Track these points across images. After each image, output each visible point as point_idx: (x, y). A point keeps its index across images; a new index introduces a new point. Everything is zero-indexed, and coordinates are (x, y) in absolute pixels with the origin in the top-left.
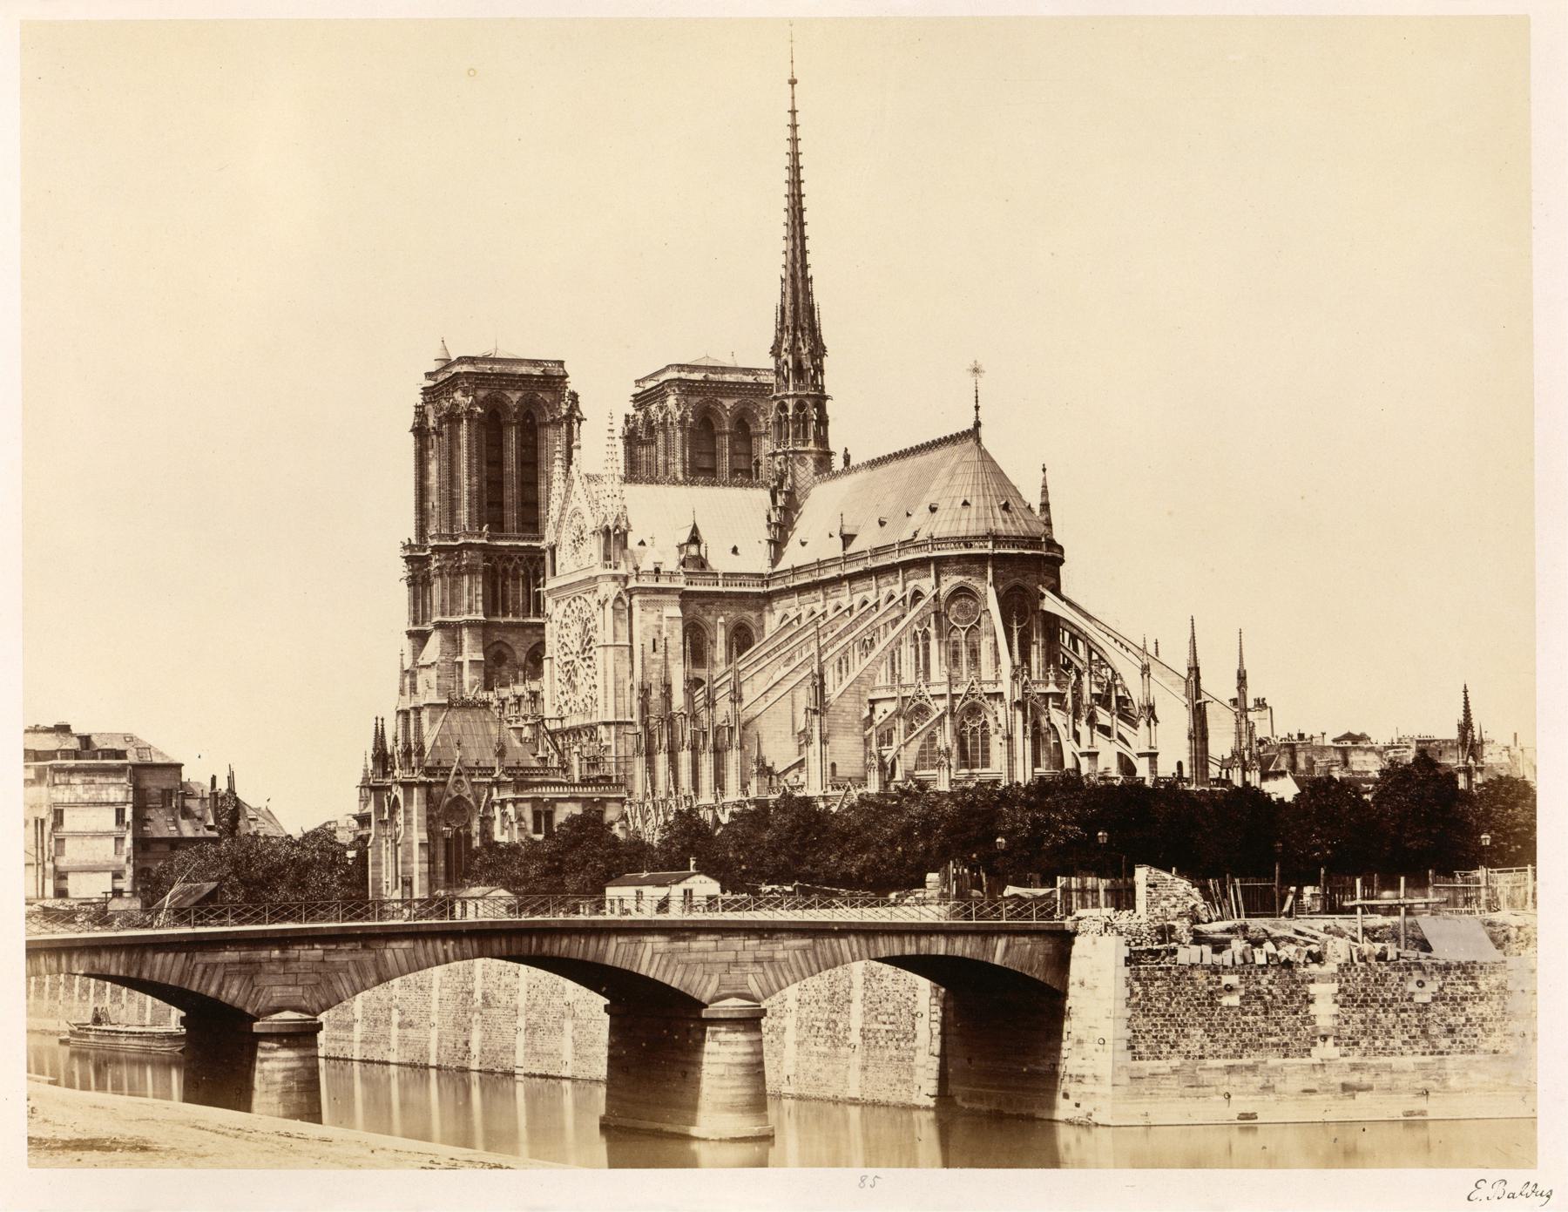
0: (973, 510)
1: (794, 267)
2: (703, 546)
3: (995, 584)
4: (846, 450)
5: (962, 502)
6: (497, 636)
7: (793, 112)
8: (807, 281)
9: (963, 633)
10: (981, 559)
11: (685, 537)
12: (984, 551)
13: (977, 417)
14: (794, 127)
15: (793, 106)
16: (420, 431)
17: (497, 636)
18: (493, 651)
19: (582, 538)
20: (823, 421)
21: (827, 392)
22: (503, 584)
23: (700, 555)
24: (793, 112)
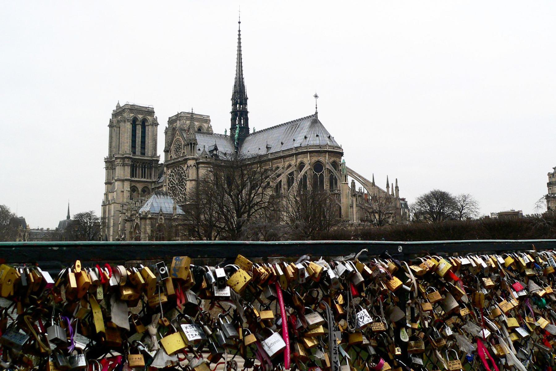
0: (320, 138)
3: (329, 160)
4: (254, 128)
5: (316, 135)
6: (133, 184)
7: (239, 31)
8: (243, 79)
9: (318, 176)
11: (213, 148)
12: (326, 149)
13: (316, 110)
16: (111, 126)
17: (133, 184)
19: (180, 148)
20: (246, 120)
21: (248, 111)
22: (136, 170)
24: (239, 31)
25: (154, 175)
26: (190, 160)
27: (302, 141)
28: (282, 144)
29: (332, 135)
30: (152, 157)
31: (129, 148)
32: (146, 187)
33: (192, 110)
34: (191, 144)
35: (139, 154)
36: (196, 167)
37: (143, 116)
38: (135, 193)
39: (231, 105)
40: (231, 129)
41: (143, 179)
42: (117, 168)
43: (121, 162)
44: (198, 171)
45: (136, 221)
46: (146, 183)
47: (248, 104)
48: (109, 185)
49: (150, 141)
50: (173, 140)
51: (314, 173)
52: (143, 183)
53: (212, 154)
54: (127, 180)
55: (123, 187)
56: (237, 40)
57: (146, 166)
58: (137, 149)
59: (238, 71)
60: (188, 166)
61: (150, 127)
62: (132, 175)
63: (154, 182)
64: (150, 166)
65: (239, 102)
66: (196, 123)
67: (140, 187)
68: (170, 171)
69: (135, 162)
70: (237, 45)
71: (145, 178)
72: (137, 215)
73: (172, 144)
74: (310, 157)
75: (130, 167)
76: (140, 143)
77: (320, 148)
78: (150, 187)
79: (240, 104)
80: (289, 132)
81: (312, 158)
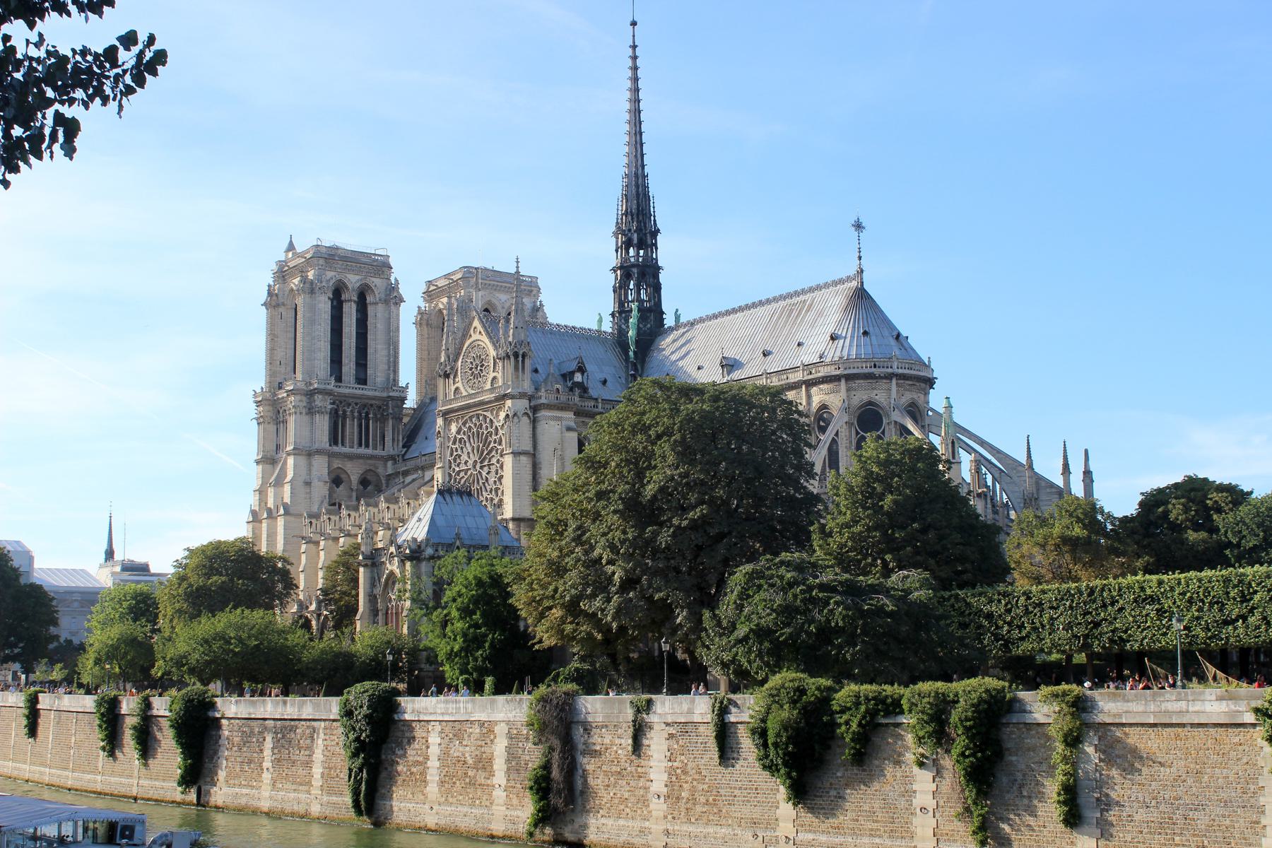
0: (873, 338)
1: (636, 167)
2: (585, 374)
4: (677, 310)
6: (337, 463)
7: (634, 47)
10: (889, 377)
11: (573, 366)
12: (890, 370)
14: (635, 58)
15: (634, 42)
17: (337, 463)
18: (333, 476)
20: (657, 288)
22: (344, 426)
23: (583, 382)
24: (634, 47)
25: (393, 440)
26: (512, 397)
27: (821, 348)
28: (765, 354)
29: (904, 334)
30: (386, 388)
31: (325, 365)
32: (370, 470)
33: (518, 262)
34: (516, 355)
35: (352, 379)
36: (529, 417)
37: (360, 277)
38: (341, 487)
39: (615, 248)
40: (613, 315)
41: (362, 450)
42: (292, 421)
43: (305, 404)
44: (534, 428)
45: (388, 565)
46: (369, 462)
47: (659, 245)
48: (269, 467)
49: (379, 347)
50: (462, 344)
51: (857, 433)
52: (361, 461)
53: (569, 384)
54: (319, 452)
55: (310, 470)
56: (629, 73)
57: (371, 416)
58: (345, 369)
59: (632, 157)
60: (507, 415)
61: (380, 307)
62: (334, 440)
63: (392, 458)
64: (382, 415)
65: (635, 241)
66: (503, 297)
67: (354, 472)
68: (454, 428)
69: (341, 402)
70: (629, 84)
71: (367, 446)
72: (392, 549)
73: (459, 354)
74: (848, 390)
75: (327, 417)
76: (353, 352)
77: (875, 366)
78: (380, 471)
79: (639, 246)
80: (782, 322)
81: (854, 393)
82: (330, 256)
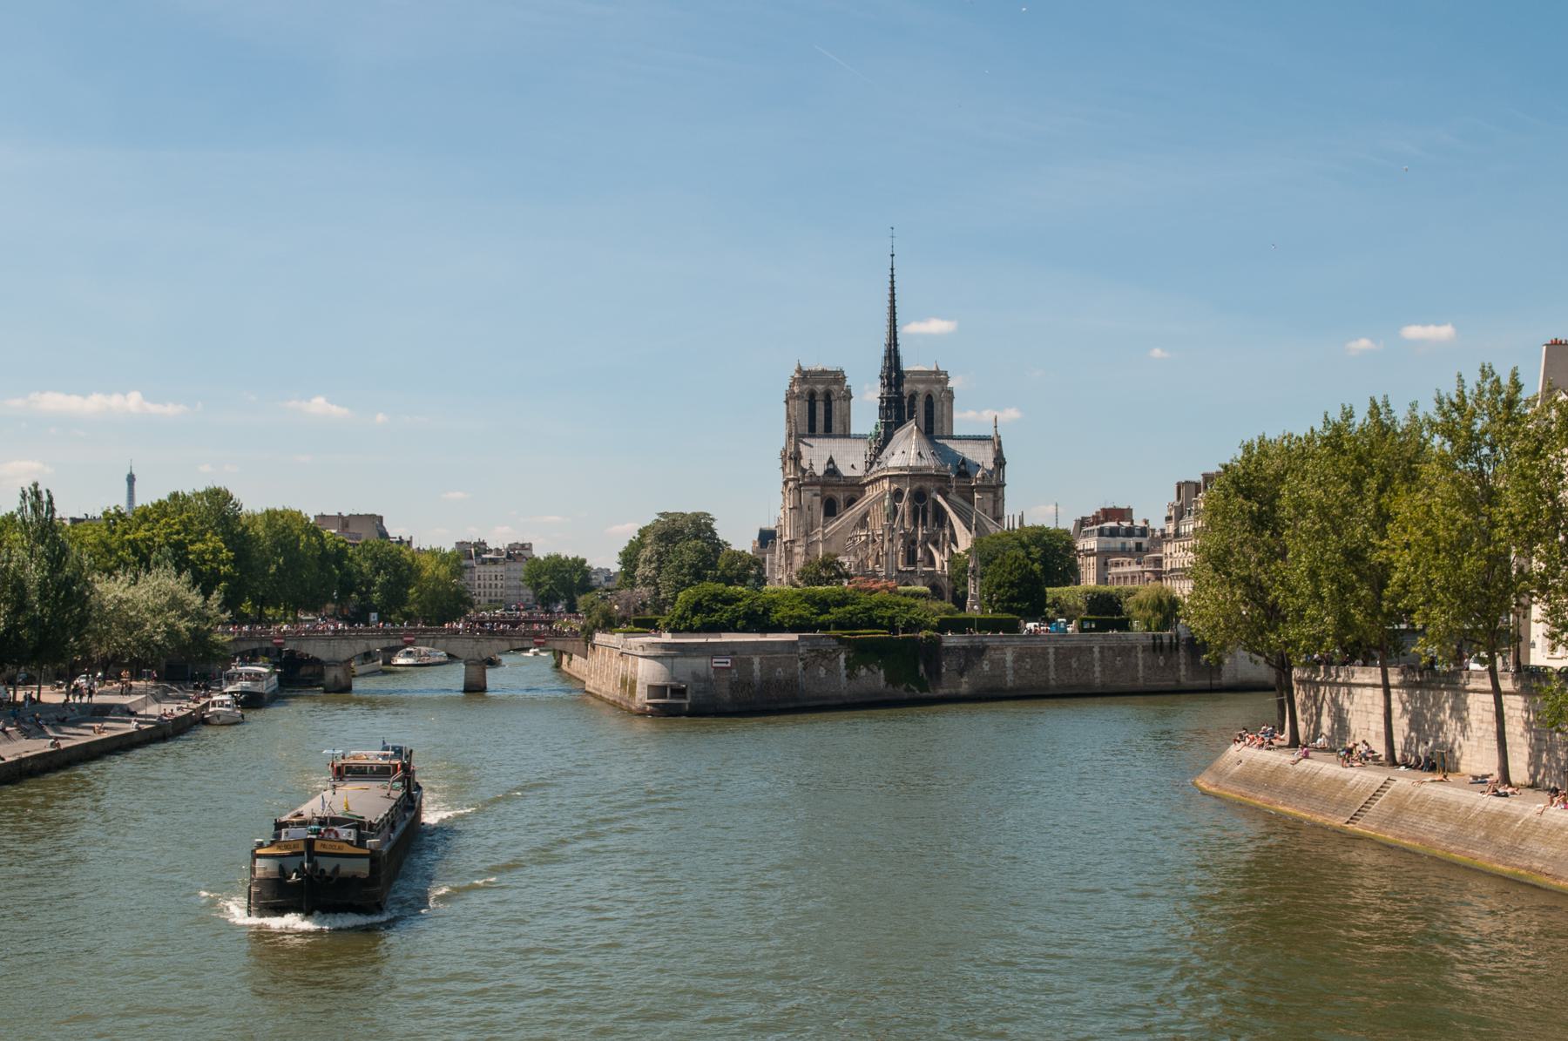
7: (892, 269)
24: (892, 269)
74: (890, 482)
82: (804, 376)
